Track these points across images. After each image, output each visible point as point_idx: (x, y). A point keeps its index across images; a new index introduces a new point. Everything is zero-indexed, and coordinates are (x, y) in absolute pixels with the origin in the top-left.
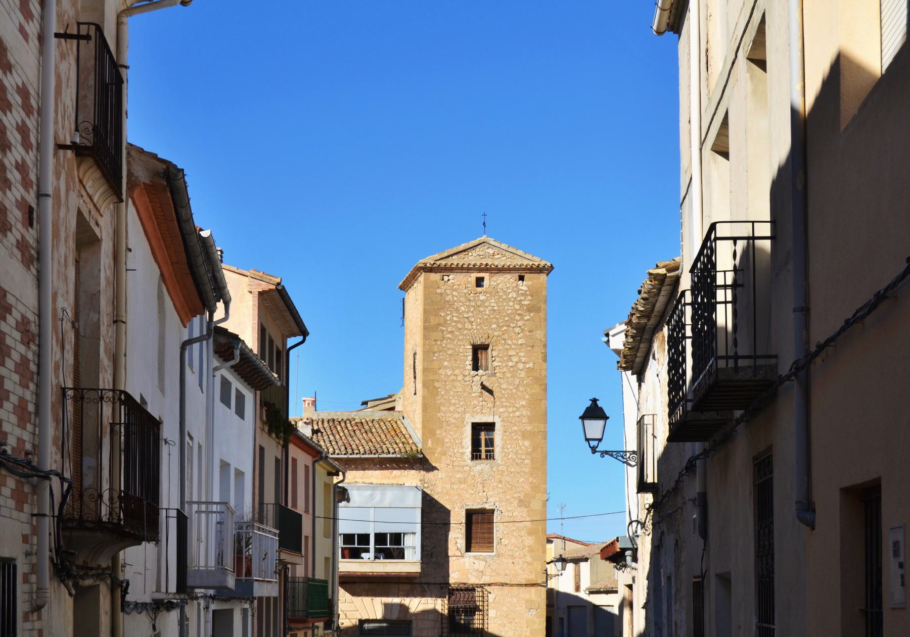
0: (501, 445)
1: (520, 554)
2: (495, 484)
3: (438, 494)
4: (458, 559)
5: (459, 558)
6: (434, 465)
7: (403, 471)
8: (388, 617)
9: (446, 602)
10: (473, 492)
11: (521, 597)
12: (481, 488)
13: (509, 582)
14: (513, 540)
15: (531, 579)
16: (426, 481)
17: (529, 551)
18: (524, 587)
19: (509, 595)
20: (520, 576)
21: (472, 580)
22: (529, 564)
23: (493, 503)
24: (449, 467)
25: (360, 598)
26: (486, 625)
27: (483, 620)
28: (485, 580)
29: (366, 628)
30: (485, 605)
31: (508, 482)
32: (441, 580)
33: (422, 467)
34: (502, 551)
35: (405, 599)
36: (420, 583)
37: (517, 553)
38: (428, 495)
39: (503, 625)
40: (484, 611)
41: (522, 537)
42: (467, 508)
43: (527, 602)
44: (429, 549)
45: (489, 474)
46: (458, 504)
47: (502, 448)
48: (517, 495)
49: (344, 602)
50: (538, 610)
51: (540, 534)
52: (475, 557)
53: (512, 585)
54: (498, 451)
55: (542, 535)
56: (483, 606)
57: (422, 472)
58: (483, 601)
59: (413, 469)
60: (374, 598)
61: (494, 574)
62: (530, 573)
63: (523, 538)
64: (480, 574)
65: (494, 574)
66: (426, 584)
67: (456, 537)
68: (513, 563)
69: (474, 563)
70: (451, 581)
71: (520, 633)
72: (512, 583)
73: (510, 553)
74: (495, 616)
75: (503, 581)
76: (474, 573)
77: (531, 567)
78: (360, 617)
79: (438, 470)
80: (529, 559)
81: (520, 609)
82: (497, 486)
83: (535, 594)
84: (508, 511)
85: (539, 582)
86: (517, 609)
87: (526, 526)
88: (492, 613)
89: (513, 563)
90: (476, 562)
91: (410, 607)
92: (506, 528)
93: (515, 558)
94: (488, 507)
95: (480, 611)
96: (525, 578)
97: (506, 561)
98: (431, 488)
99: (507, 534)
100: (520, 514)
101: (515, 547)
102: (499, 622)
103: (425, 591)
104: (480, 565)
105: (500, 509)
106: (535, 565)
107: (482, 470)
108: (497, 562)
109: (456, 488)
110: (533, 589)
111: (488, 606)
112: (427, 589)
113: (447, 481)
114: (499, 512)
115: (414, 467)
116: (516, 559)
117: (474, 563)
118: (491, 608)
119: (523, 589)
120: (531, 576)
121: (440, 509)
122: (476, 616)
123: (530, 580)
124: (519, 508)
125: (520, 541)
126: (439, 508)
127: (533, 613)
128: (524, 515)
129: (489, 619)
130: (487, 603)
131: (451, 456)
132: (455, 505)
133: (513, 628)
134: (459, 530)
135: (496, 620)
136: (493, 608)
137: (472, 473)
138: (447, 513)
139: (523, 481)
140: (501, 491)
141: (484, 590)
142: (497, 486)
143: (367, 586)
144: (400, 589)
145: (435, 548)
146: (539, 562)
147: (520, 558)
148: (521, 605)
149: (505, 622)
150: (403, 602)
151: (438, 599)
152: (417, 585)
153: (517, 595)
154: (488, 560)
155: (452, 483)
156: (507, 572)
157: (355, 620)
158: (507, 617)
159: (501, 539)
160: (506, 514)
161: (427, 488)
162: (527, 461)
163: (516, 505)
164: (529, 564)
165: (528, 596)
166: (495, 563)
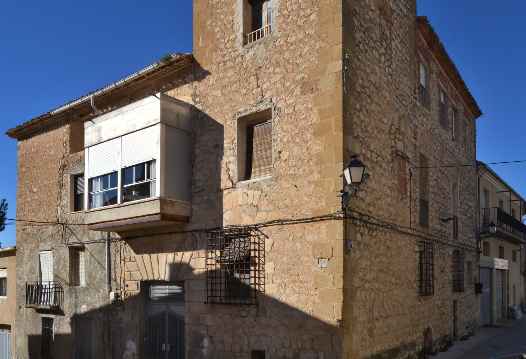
0: (278, 7)
1: (304, 170)
2: (271, 70)
3: (208, 107)
4: (230, 193)
5: (230, 190)
6: (205, 69)
7: (176, 89)
10: (245, 91)
11: (307, 240)
12: (254, 83)
13: (289, 217)
14: (296, 150)
15: (321, 208)
16: (197, 94)
17: (316, 164)
18: (311, 223)
19: (290, 239)
20: (305, 206)
21: (246, 221)
22: (317, 184)
23: (269, 100)
24: (220, 65)
25: (141, 255)
26: (262, 286)
27: (259, 278)
28: (261, 217)
30: (261, 255)
31: (289, 60)
32: (211, 225)
33: (193, 77)
34: (281, 171)
35: (177, 253)
36: (191, 231)
37: (300, 170)
38: (199, 111)
39: (284, 285)
40: (259, 264)
41: (306, 142)
42: (239, 117)
43: (314, 246)
44: (201, 184)
45: (264, 56)
46: (230, 114)
47: (280, 11)
48: (299, 77)
49: (129, 261)
50: (331, 260)
51: (333, 131)
52: (248, 185)
53: (293, 222)
54: (275, 17)
55: (335, 131)
56: (259, 257)
57: (195, 84)
58: (259, 251)
59: (186, 83)
60: (152, 255)
61: (271, 207)
62: (319, 198)
63: (308, 145)
64: (255, 210)
65: (271, 207)
66: (195, 231)
67: (228, 161)
68: (295, 186)
69: (247, 195)
70: (225, 224)
71: (306, 297)
72: (295, 218)
73: (291, 172)
74: (272, 271)
75: (281, 218)
76: (248, 210)
77: (321, 189)
78: (140, 278)
79: (210, 74)
80: (316, 176)
81: (306, 259)
82: (274, 72)
83: (327, 232)
84: (288, 106)
85: (332, 212)
86: (302, 259)
87: (312, 123)
88: (269, 267)
89: (295, 186)
90: (250, 192)
92: (285, 134)
93: (297, 178)
94: (262, 107)
95: (255, 264)
96: (311, 209)
97: (285, 185)
98: (202, 101)
99: (287, 142)
100: (305, 105)
101: (298, 160)
102: (279, 281)
104: (254, 196)
105: (278, 106)
106: (326, 184)
107: (254, 54)
108: (275, 188)
109: (228, 93)
110: (323, 225)
111: (264, 257)
112: (198, 238)
113: (219, 86)
114: (276, 111)
115: (186, 80)
116: (299, 180)
117: (247, 195)
118: (268, 260)
119: (308, 226)
120: (320, 204)
121: (211, 127)
122: (253, 273)
123: (319, 210)
124: (303, 97)
125: (305, 150)
126: (210, 126)
127: (324, 266)
128: (310, 106)
129: (266, 276)
130: (262, 252)
131: (222, 50)
132: (227, 117)
133: (297, 291)
134: (232, 150)
135: (274, 278)
136: (271, 261)
137: (244, 65)
138: (220, 129)
139: (308, 51)
140: (279, 76)
141: (260, 233)
142: (274, 72)
143: (145, 240)
145: (206, 181)
146: (332, 179)
147: (305, 177)
148: (306, 252)
149: (286, 280)
152: (189, 234)
153: (301, 237)
154: (264, 186)
155: (224, 87)
156: (288, 201)
158: (288, 273)
159: (280, 152)
160: (286, 111)
161: (198, 103)
162: (313, 17)
163: (299, 94)
164: (317, 184)
165: (316, 237)
166: (272, 191)
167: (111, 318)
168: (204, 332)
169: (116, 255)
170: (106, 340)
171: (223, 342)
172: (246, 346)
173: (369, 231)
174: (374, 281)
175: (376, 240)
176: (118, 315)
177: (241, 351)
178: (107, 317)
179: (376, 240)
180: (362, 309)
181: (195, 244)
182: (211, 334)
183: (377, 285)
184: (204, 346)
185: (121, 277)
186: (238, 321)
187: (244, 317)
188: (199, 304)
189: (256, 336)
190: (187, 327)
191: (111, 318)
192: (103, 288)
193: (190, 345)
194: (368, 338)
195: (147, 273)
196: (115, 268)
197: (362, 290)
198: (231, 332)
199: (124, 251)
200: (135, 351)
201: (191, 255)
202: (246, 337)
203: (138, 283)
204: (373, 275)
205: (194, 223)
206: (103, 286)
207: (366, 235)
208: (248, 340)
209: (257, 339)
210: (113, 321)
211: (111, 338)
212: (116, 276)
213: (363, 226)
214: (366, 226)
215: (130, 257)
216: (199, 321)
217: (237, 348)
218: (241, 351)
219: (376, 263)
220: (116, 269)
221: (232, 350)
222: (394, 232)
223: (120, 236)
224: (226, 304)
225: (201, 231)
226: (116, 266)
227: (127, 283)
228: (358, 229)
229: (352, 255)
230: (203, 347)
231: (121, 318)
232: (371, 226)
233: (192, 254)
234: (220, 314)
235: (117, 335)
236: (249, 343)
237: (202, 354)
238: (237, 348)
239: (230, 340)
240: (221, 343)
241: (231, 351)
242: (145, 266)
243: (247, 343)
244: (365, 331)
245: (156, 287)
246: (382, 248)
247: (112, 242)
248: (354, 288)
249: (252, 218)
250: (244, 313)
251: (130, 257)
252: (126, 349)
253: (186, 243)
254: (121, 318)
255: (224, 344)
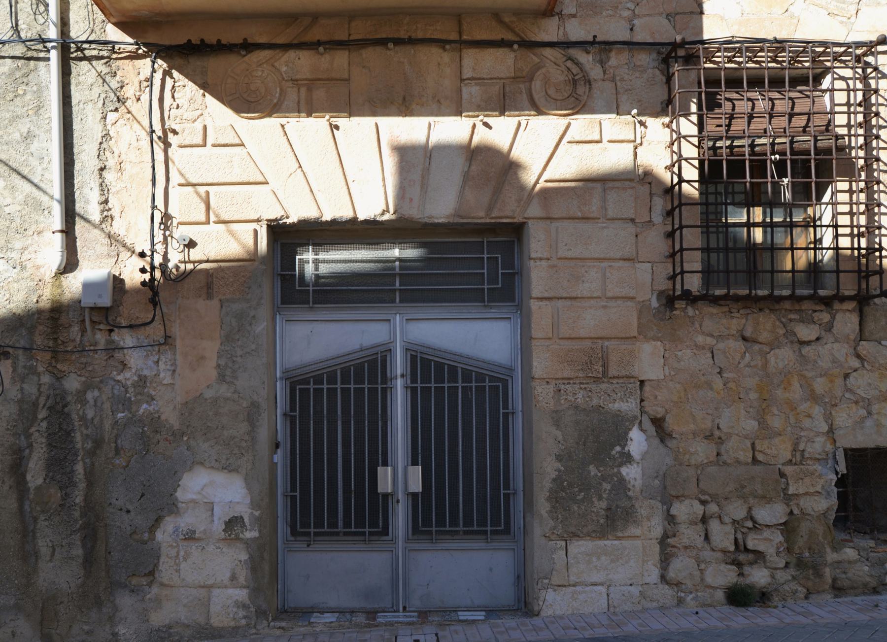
8: (414, 212)
9: (688, 127)
25: (272, 123)
29: (309, 269)
36: (566, 44)
49: (199, 141)
78: (274, 213)
91: (517, 154)
103: (589, 82)
112: (595, 72)
144: (467, 73)
150: (482, 136)
151: (650, 121)
152: (548, 52)
157: (255, 225)
167: (73, 383)
168: (628, 406)
169: (111, 117)
170: (35, 476)
171: (717, 433)
172: (820, 440)
176: (124, 366)
177: (798, 457)
178: (46, 379)
181: (581, 90)
182: (659, 412)
184: (632, 453)
185: (154, 207)
186: (784, 356)
187: (808, 343)
188: (605, 307)
189: (856, 403)
190: (543, 393)
191: (73, 383)
192: (15, 255)
193: (559, 458)
195: (312, 191)
196: (102, 169)
198: (753, 396)
199: (161, 100)
200: (244, 510)
201: (564, 128)
202: (817, 411)
203: (256, 232)
205: (574, 16)
206: (18, 245)
208: (829, 418)
209: (863, 412)
210: (90, 396)
211: (79, 468)
212: (106, 202)
215: (205, 128)
216: (605, 366)
217: (781, 450)
218: (798, 457)
220: (109, 176)
221: (760, 457)
223: (133, 38)
224: (715, 300)
225: (606, 46)
226: (111, 163)
227: (180, 232)
230: (627, 459)
231: (142, 381)
233: (568, 127)
234: (700, 339)
235: (117, 451)
236: (831, 430)
237: (621, 484)
238: (781, 450)
239: (751, 425)
240: (709, 437)
241: (755, 460)
242: (300, 167)
243: (825, 428)
245: (322, 256)
247: (80, 59)
249: (842, 22)
250: (805, 332)
251: (205, 128)
252: (172, 507)
253: (537, 85)
254: (142, 381)
255: (721, 441)
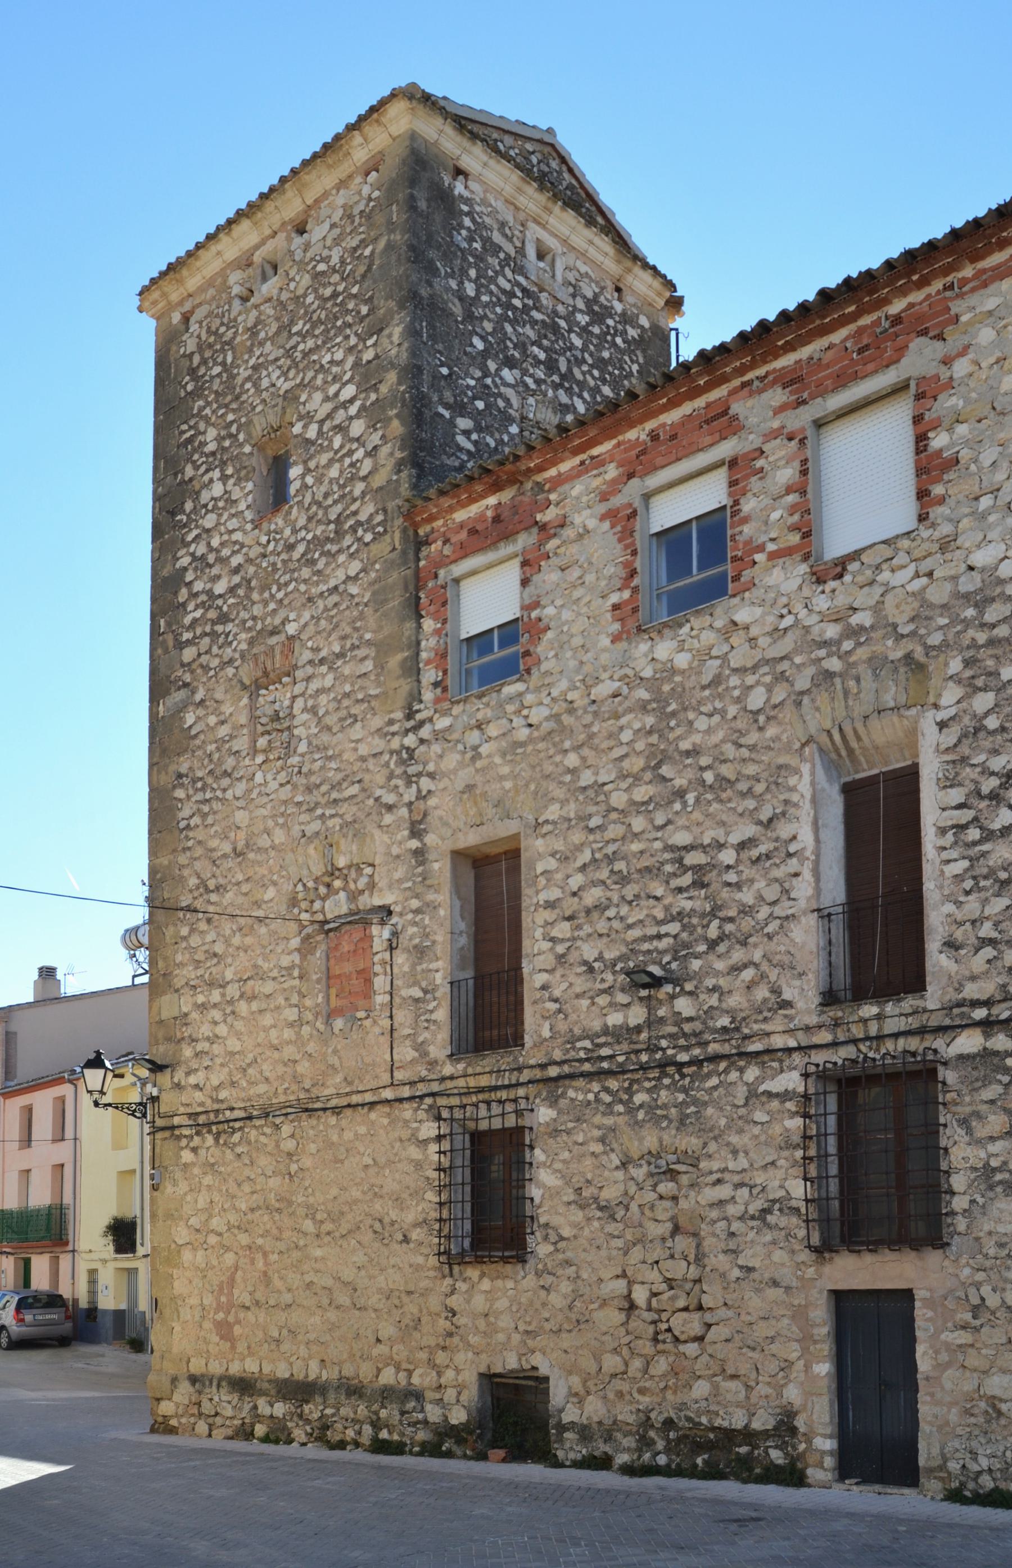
173: (217, 1139)
174: (236, 1231)
175: (239, 1150)
179: (239, 1150)
180: (196, 1281)
183: (244, 1239)
194: (216, 1339)
197: (195, 1249)
204: (233, 1218)
207: (208, 1148)
213: (198, 1133)
214: (209, 1132)
219: (240, 1194)
222: (310, 1116)
228: (184, 1142)
229: (169, 1189)
232: (221, 1127)
244: (207, 1325)
246: (263, 1161)
248: (173, 1246)
